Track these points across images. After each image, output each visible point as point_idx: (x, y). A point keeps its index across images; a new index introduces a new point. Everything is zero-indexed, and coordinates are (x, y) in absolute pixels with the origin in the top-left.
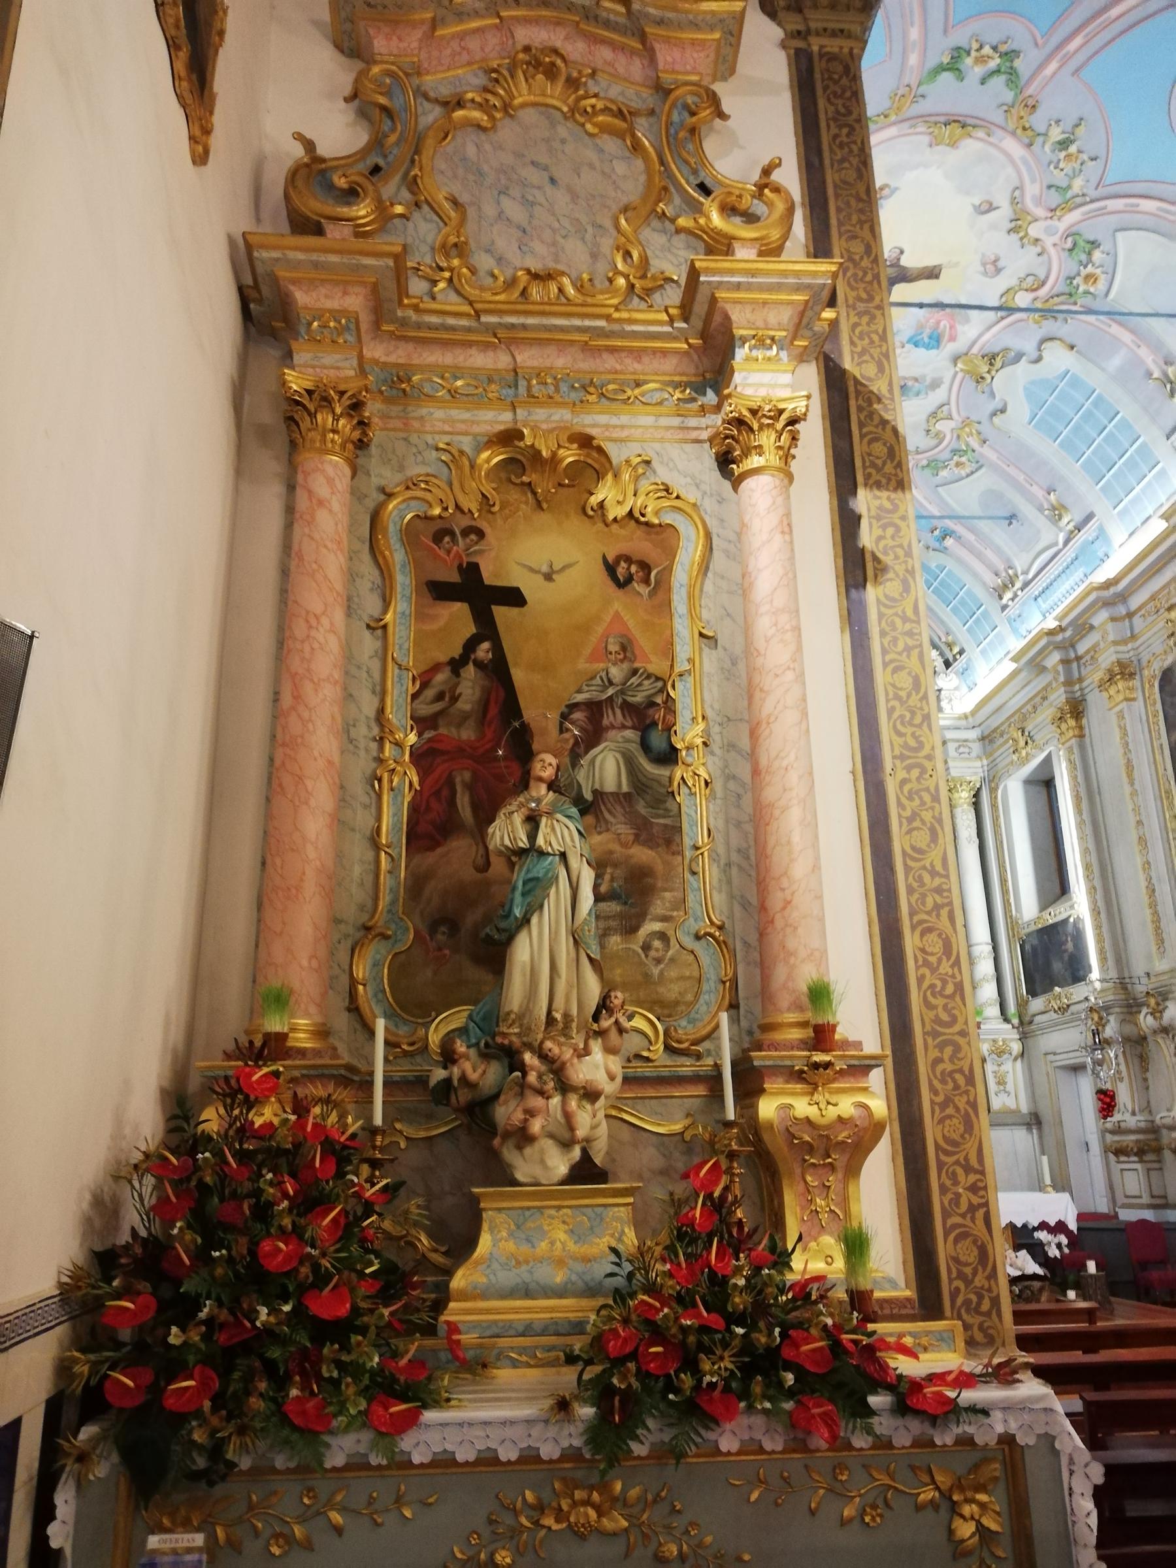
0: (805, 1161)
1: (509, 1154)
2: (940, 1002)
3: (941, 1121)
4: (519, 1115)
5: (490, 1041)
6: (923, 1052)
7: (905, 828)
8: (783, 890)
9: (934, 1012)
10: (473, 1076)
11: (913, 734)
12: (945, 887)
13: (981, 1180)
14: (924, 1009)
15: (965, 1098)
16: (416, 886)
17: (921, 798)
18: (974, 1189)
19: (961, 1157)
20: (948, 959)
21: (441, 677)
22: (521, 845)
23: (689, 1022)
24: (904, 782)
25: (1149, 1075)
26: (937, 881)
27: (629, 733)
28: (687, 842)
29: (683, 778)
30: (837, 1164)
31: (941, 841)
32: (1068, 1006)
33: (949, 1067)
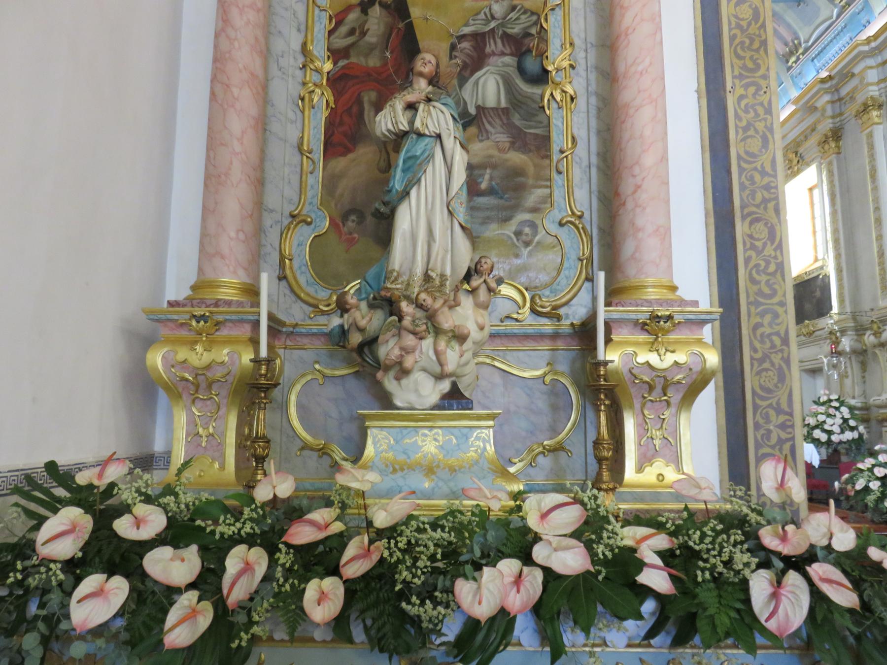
0: (645, 398)
1: (389, 383)
2: (763, 278)
3: (758, 373)
4: (397, 352)
5: (377, 295)
6: (746, 318)
7: (740, 137)
8: (634, 176)
9: (758, 287)
10: (362, 323)
11: (751, 58)
12: (773, 185)
13: (790, 420)
14: (749, 284)
15: (780, 355)
16: (330, 184)
17: (755, 111)
18: (783, 426)
19: (774, 401)
20: (772, 243)
21: (353, 16)
22: (402, 128)
23: (551, 292)
24: (741, 98)
25: (866, 374)
26: (766, 180)
27: (508, 59)
28: (555, 148)
29: (552, 94)
30: (672, 401)
31: (771, 146)
32: (814, 332)
33: (768, 330)
